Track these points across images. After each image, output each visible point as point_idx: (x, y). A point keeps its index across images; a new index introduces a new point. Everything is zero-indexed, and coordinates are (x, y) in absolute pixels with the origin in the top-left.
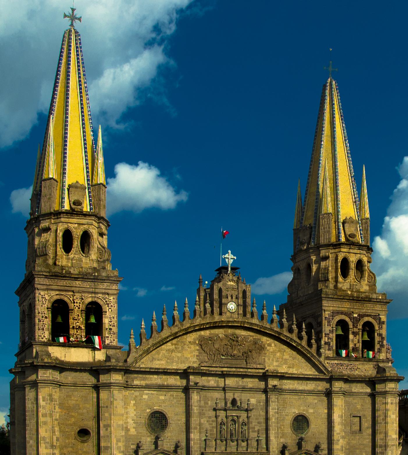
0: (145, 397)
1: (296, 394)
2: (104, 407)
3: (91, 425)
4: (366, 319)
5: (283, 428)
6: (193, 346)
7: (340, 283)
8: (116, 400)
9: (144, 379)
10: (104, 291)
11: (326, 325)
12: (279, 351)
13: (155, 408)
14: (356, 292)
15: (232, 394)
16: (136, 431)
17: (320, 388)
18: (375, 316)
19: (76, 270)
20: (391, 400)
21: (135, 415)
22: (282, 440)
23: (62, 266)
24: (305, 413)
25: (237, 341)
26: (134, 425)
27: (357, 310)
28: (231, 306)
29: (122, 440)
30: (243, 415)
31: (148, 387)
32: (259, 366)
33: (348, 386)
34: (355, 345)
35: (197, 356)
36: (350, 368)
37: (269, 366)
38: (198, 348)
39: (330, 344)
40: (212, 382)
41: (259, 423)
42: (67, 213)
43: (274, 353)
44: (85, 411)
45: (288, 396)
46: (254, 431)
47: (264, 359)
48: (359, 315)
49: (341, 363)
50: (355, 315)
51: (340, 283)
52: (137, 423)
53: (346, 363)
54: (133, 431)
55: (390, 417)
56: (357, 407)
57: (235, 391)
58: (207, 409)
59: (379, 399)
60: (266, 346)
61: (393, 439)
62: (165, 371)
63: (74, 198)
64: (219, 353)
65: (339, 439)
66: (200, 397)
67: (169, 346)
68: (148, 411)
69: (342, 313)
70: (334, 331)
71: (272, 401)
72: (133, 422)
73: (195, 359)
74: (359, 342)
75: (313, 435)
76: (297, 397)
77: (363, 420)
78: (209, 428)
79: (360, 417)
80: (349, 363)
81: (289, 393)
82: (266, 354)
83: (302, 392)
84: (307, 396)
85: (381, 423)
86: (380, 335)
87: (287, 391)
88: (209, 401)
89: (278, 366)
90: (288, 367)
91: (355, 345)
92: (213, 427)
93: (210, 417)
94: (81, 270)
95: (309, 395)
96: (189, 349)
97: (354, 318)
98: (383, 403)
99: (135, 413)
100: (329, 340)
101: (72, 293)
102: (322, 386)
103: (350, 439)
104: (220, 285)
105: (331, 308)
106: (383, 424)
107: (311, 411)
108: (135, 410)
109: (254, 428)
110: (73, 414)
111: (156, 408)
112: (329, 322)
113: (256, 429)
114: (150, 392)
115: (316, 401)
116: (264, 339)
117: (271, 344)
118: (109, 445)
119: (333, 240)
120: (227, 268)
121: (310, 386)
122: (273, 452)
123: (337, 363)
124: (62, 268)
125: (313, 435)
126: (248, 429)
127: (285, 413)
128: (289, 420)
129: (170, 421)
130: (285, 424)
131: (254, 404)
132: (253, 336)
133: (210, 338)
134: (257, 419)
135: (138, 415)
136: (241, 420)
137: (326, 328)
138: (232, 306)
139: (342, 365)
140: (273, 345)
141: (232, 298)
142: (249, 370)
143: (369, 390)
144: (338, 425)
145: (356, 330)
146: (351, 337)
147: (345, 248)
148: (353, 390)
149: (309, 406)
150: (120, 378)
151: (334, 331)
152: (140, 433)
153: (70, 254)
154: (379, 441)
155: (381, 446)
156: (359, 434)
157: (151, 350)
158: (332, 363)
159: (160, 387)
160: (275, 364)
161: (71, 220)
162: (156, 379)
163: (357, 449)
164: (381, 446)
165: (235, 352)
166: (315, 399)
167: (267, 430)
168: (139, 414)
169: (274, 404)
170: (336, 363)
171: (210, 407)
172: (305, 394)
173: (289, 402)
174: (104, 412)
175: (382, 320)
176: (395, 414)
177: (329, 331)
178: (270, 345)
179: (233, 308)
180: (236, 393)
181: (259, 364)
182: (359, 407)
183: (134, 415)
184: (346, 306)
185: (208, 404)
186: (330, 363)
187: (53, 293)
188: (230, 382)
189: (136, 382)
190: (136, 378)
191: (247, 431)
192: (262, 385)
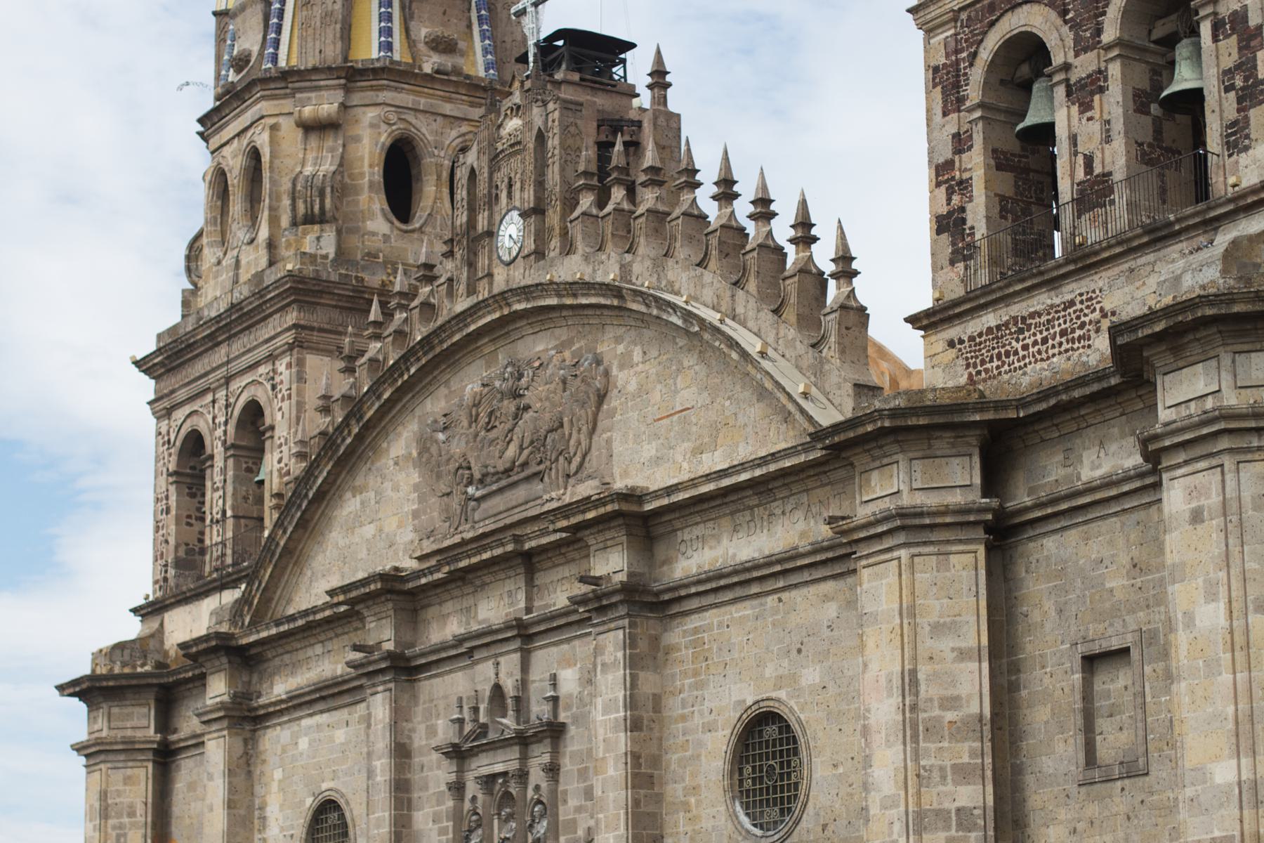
1: (739, 592)
5: (698, 803)
10: (263, 352)
20: (1191, 493)
24: (782, 694)
25: (516, 395)
33: (1060, 457)
34: (1089, 161)
35: (416, 514)
36: (1063, 333)
43: (642, 391)
45: (711, 617)
47: (609, 442)
49: (1015, 318)
53: (1039, 308)
56: (1108, 585)
60: (615, 371)
65: (895, 836)
68: (309, 801)
75: (824, 827)
76: (745, 610)
79: (1125, 651)
80: (1057, 301)
81: (711, 599)
84: (794, 593)
87: (693, 590)
88: (438, 716)
89: (657, 460)
91: (1089, 161)
95: (796, 586)
100: (956, 199)
101: (209, 397)
103: (1080, 826)
107: (811, 675)
123: (993, 323)
125: (824, 827)
127: (701, 713)
130: (702, 783)
131: (571, 695)
139: (1021, 325)
141: (510, 186)
145: (1085, 65)
149: (799, 651)
156: (1127, 782)
157: (282, 543)
158: (972, 339)
166: (826, 598)
169: (610, 677)
170: (990, 330)
176: (1223, 591)
178: (626, 363)
180: (502, 654)
182: (1117, 582)
186: (961, 342)
187: (180, 414)
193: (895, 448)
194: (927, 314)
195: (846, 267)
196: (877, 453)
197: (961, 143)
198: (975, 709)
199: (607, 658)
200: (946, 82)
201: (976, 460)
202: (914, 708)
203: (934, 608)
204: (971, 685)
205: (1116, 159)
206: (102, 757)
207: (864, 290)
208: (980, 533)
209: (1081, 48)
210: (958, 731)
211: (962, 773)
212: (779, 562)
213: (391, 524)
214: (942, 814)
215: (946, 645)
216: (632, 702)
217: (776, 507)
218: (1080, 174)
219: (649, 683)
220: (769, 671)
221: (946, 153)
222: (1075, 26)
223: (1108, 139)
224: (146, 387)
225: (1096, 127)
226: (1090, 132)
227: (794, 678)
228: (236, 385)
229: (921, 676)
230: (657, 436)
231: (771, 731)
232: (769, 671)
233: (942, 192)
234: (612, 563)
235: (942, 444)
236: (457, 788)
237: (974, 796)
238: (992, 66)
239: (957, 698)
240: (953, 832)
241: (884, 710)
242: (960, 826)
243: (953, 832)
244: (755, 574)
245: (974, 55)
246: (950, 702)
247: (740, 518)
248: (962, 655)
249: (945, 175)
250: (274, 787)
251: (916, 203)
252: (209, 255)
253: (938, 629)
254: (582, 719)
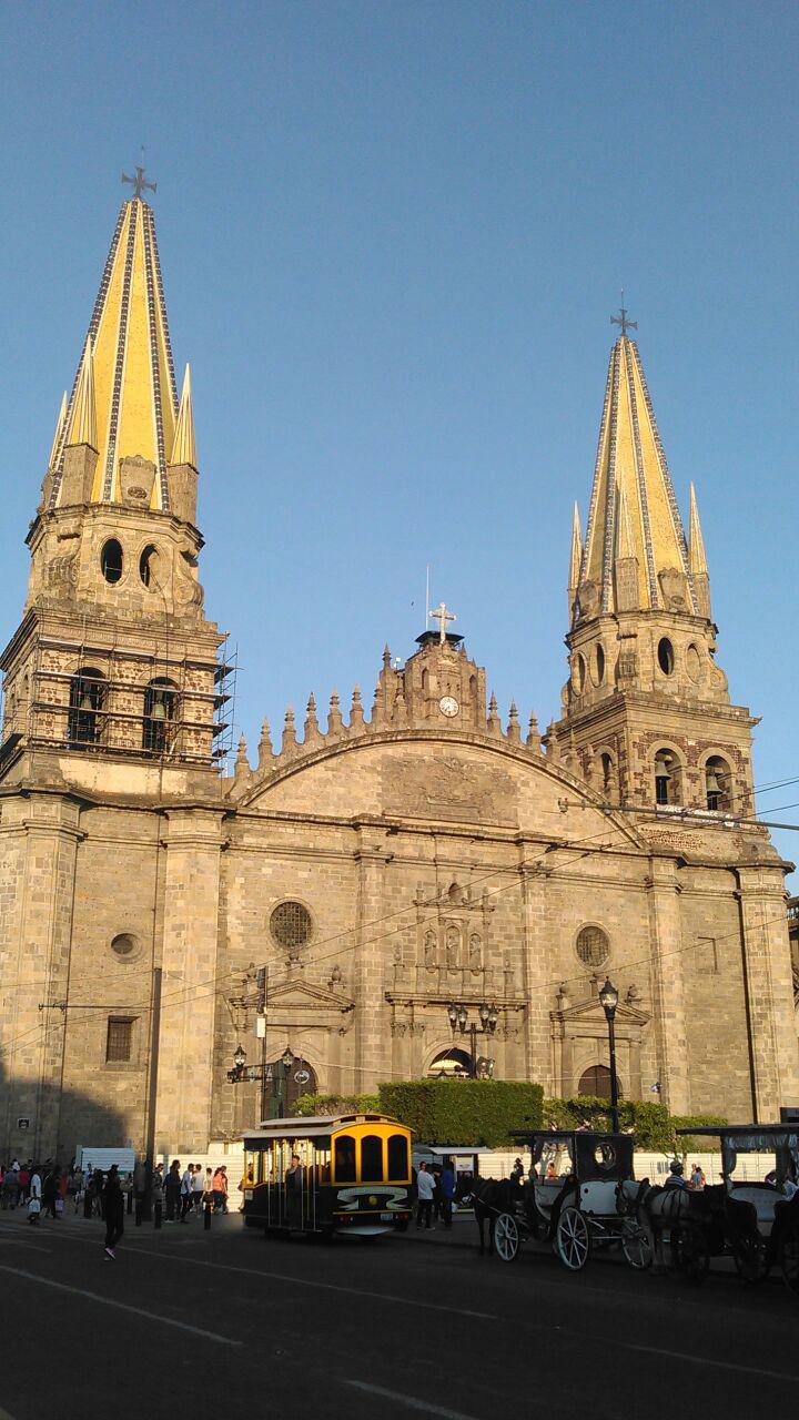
0: (265, 870)
2: (174, 887)
3: (140, 924)
4: (713, 751)
6: (370, 775)
7: (660, 682)
8: (202, 872)
9: (265, 835)
11: (636, 757)
12: (545, 796)
13: (287, 895)
14: (689, 700)
15: (450, 874)
16: (243, 941)
17: (629, 875)
18: (730, 746)
19: (128, 613)
21: (243, 908)
22: (556, 976)
23: (99, 605)
24: (600, 922)
26: (241, 929)
27: (694, 732)
28: (448, 704)
29: (211, 958)
30: (476, 918)
31: (274, 850)
32: (504, 823)
35: (378, 795)
37: (526, 825)
38: (380, 779)
39: (645, 793)
40: (406, 846)
41: (508, 937)
42: (114, 507)
43: (534, 798)
44: (132, 896)
46: (498, 955)
47: (516, 810)
48: (698, 743)
51: (660, 682)
52: (247, 924)
54: (236, 942)
55: (772, 940)
57: (456, 869)
58: (399, 902)
59: (748, 905)
60: (519, 785)
61: (784, 988)
62: (312, 819)
63: (130, 483)
64: (424, 793)
66: (384, 878)
67: (318, 771)
69: (666, 737)
70: (653, 771)
71: (533, 894)
72: (239, 921)
73: (374, 801)
76: (582, 889)
77: (720, 946)
78: (402, 944)
82: (519, 800)
83: (593, 879)
85: (756, 954)
86: (743, 783)
88: (402, 885)
90: (564, 830)
92: (411, 941)
93: (404, 920)
94: (139, 615)
96: (361, 781)
97: (690, 748)
98: (757, 914)
99: (244, 905)
102: (634, 870)
104: (425, 663)
105: (645, 726)
106: (760, 957)
107: (613, 919)
108: (243, 897)
109: (497, 947)
110: (105, 901)
111: (290, 896)
112: (642, 752)
113: (501, 951)
114: (278, 862)
115: (622, 901)
116: (516, 771)
117: (528, 783)
118: (183, 969)
119: (645, 606)
120: (437, 635)
121: (609, 868)
122: (538, 998)
124: (100, 608)
126: (487, 947)
128: (569, 937)
129: (316, 922)
132: (492, 765)
133: (406, 764)
134: (501, 929)
135: (250, 909)
136: (469, 928)
137: (636, 764)
138: (449, 705)
139: (669, 834)
140: (531, 784)
142: (486, 829)
143: (728, 885)
145: (692, 770)
146: (686, 782)
147: (664, 620)
150: (214, 828)
151: (653, 771)
152: (253, 947)
153: (117, 584)
154: (754, 993)
155: (759, 1002)
157: (282, 776)
159: (301, 852)
160: (539, 821)
161: (123, 522)
162: (291, 835)
163: (711, 1005)
164: (759, 1002)
165: (456, 793)
166: (620, 896)
167: (524, 952)
168: (251, 906)
171: (404, 898)
172: (601, 885)
173: (569, 900)
174: (175, 898)
177: (641, 769)
178: (525, 784)
179: (451, 709)
181: (506, 819)
183: (238, 908)
184: (673, 724)
185: (400, 892)
188: (447, 849)
189: (248, 840)
190: (248, 831)
191: (482, 953)
192: (512, 856)
206: (57, 833)
217: (606, 861)
220: (594, 913)
230: (544, 817)
231: (591, 932)
232: (594, 913)
236: (420, 919)
250: (237, 886)
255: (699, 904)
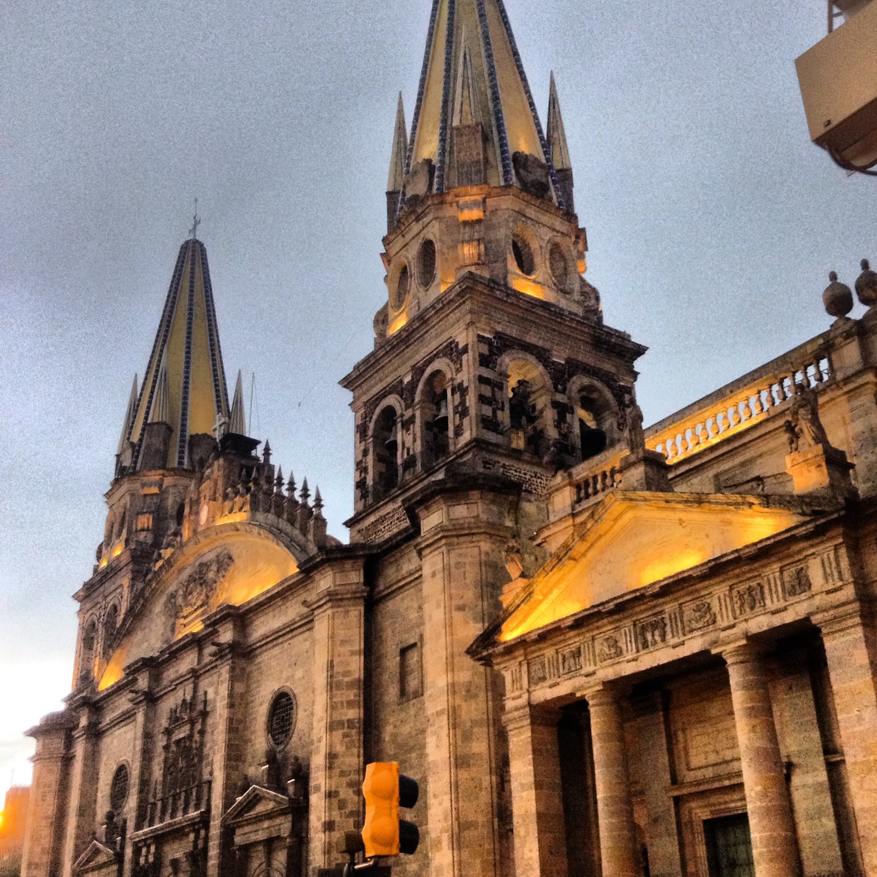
24: (288, 684)
35: (163, 635)
36: (398, 519)
50: (407, 379)
74: (414, 441)
76: (276, 651)
91: (408, 449)
100: (363, 475)
125: (300, 739)
139: (382, 519)
144: (321, 694)
145: (408, 414)
148: (404, 572)
170: (372, 523)
175: (461, 346)
193: (329, 569)
194: (351, 520)
195: (319, 504)
196: (323, 572)
197: (365, 453)
198: (356, 676)
199: (222, 679)
200: (361, 430)
201: (362, 572)
202: (331, 676)
203: (341, 634)
204: (356, 666)
205: (418, 447)
207: (325, 513)
208: (362, 601)
209: (407, 408)
210: (350, 686)
211: (350, 704)
212: (288, 626)
213: (153, 641)
214: (341, 724)
215: (345, 649)
216: (231, 696)
218: (405, 456)
219: (240, 688)
221: (360, 458)
222: (405, 400)
223: (414, 441)
224: (77, 606)
225: (411, 437)
226: (409, 439)
227: (293, 676)
228: (108, 599)
229: (335, 662)
232: (284, 676)
233: (358, 473)
234: (226, 635)
235: (348, 565)
237: (354, 714)
238: (377, 421)
239: (349, 672)
240: (346, 730)
241: (320, 679)
242: (349, 727)
243: (346, 730)
244: (281, 633)
245: (371, 418)
246: (347, 673)
247: (277, 611)
248: (353, 653)
249: (361, 467)
251: (349, 478)
252: (104, 551)
253: (343, 642)
254: (214, 710)
255: (403, 600)
